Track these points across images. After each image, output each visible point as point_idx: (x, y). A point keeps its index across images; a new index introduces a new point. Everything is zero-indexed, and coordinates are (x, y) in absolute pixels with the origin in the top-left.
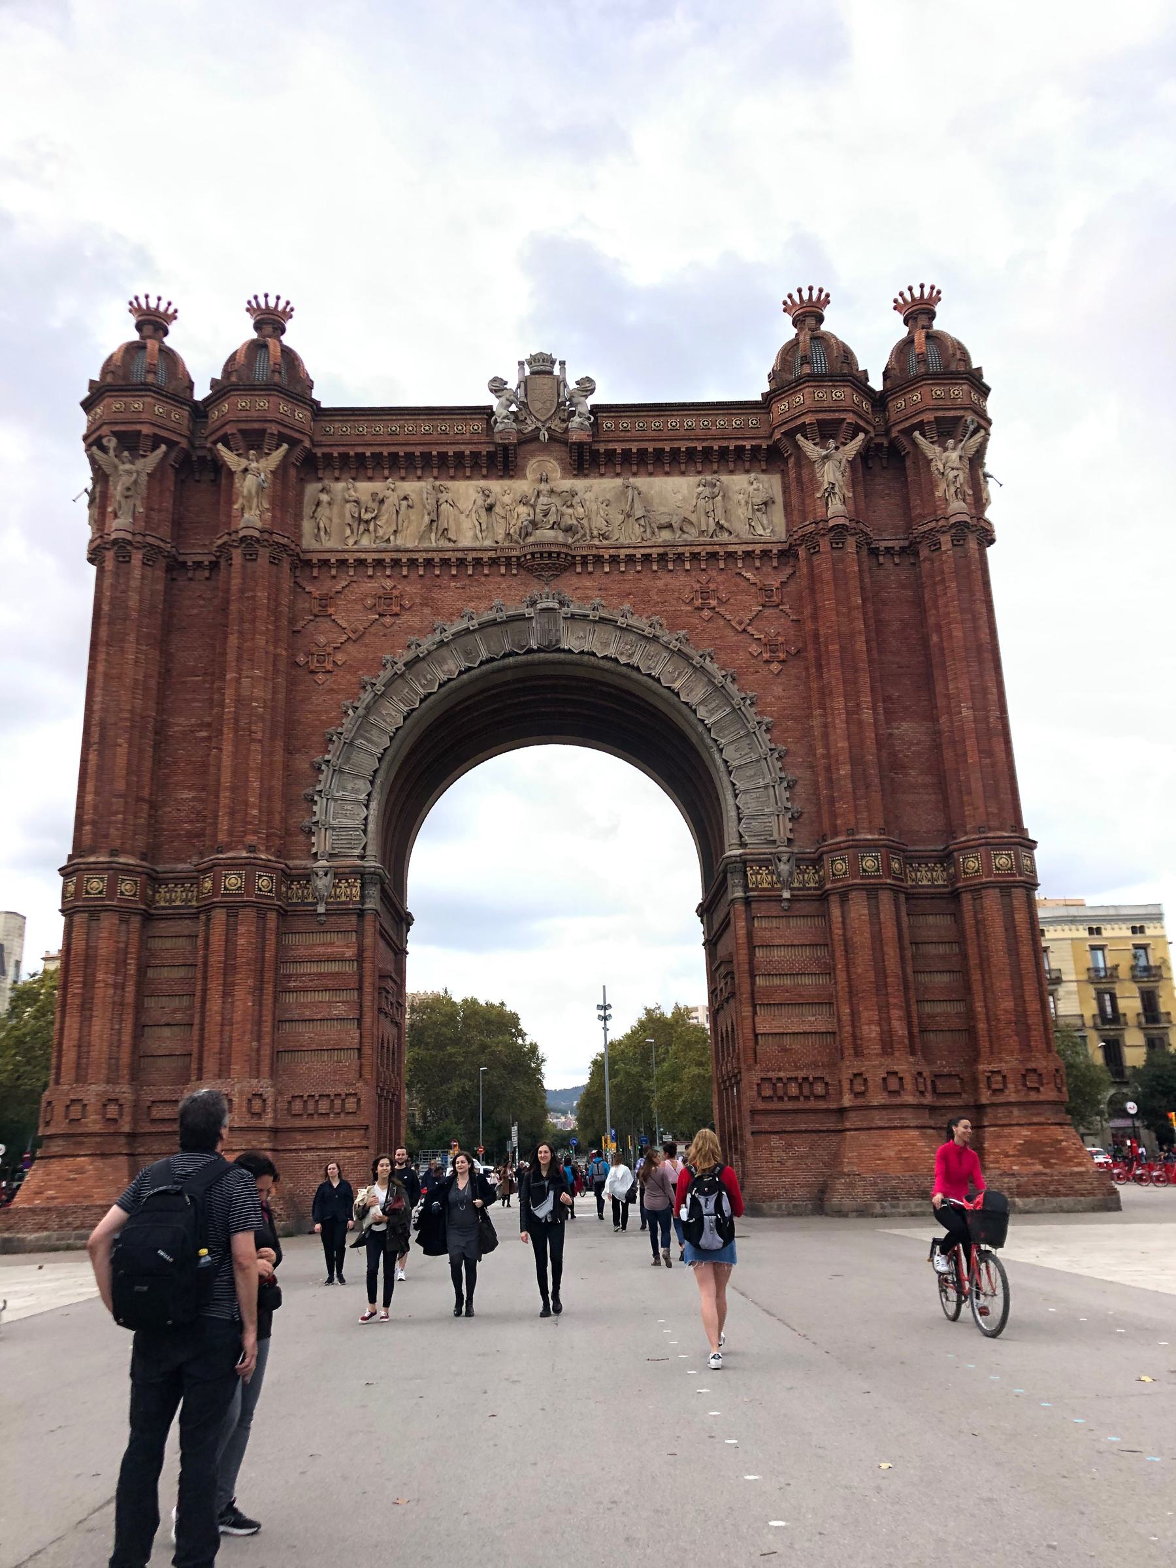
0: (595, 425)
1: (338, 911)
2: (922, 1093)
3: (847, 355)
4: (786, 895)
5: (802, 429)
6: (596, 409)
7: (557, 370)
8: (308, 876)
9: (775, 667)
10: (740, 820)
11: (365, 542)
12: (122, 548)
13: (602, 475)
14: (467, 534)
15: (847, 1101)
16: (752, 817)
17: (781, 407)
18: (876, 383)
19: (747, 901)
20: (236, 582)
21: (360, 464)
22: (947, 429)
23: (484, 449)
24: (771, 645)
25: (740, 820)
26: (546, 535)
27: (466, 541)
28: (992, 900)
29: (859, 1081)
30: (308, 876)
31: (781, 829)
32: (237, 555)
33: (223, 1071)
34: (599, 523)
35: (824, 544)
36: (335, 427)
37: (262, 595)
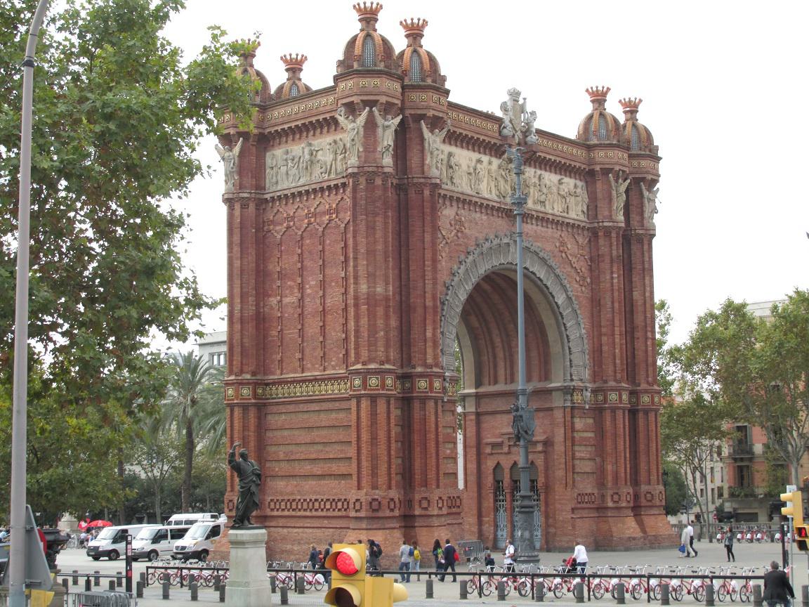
2: (629, 502)
4: (587, 407)
7: (521, 102)
9: (583, 289)
10: (571, 367)
13: (530, 166)
15: (610, 504)
16: (576, 366)
17: (600, 155)
19: (573, 408)
23: (499, 143)
25: (571, 367)
28: (652, 416)
29: (616, 497)
31: (587, 374)
32: (427, 193)
33: (438, 486)
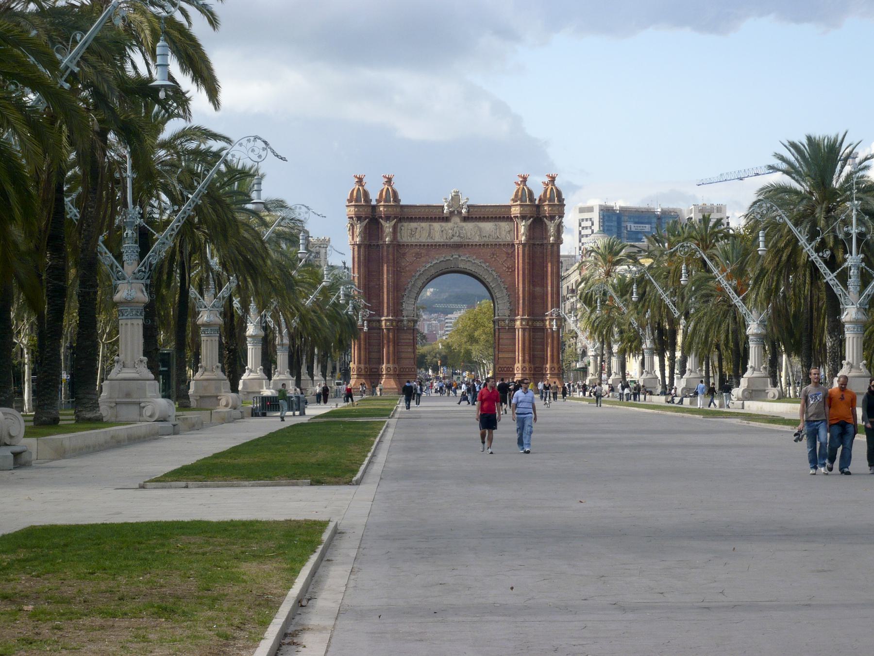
0: (468, 212)
1: (409, 329)
3: (531, 193)
5: (516, 217)
6: (468, 206)
8: (402, 321)
11: (413, 240)
12: (359, 246)
14: (438, 238)
18: (537, 202)
20: (385, 254)
21: (411, 219)
22: (552, 218)
24: (508, 268)
26: (456, 239)
27: (436, 240)
30: (402, 321)
31: (507, 313)
34: (469, 234)
35: (521, 246)
36: (405, 210)
37: (391, 257)
